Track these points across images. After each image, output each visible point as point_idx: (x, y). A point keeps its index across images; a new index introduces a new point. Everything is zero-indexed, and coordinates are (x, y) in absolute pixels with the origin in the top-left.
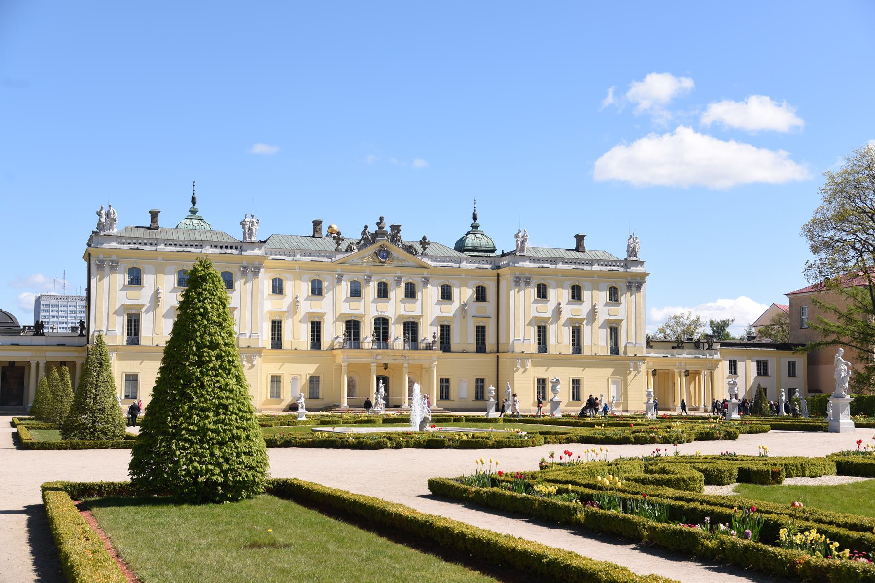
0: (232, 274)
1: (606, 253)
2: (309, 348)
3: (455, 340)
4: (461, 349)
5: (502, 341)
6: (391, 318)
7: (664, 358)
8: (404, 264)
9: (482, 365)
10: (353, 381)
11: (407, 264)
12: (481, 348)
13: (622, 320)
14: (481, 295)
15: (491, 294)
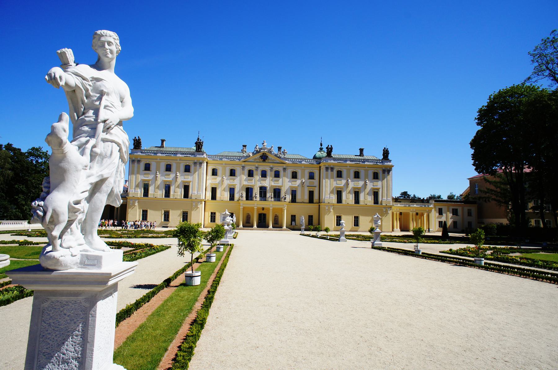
1: (374, 157)
2: (229, 200)
3: (299, 197)
4: (301, 202)
5: (321, 198)
6: (267, 187)
7: (404, 207)
8: (274, 162)
9: (311, 209)
10: (249, 215)
11: (276, 162)
12: (311, 201)
13: (380, 188)
14: (311, 176)
15: (316, 176)
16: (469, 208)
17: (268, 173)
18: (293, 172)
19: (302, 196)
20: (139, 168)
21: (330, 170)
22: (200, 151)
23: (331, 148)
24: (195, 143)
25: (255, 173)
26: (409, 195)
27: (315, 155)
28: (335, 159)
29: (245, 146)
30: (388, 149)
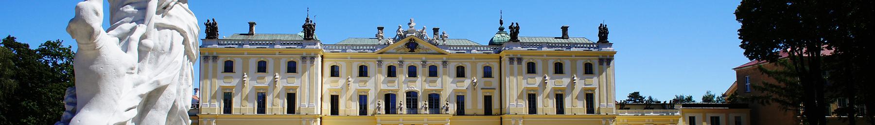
0: (296, 62)
1: (585, 39)
2: (358, 115)
3: (468, 107)
4: (472, 113)
5: (503, 107)
6: (419, 91)
7: (636, 116)
8: (428, 52)
11: (430, 52)
12: (488, 111)
13: (596, 88)
14: (487, 73)
15: (495, 72)
16: (737, 115)
17: (420, 70)
18: (458, 68)
19: (474, 104)
20: (215, 69)
21: (516, 63)
22: (310, 39)
23: (518, 28)
24: (303, 27)
25: (398, 70)
26: (641, 97)
27: (492, 39)
28: (523, 45)
29: (381, 29)
30: (606, 25)
